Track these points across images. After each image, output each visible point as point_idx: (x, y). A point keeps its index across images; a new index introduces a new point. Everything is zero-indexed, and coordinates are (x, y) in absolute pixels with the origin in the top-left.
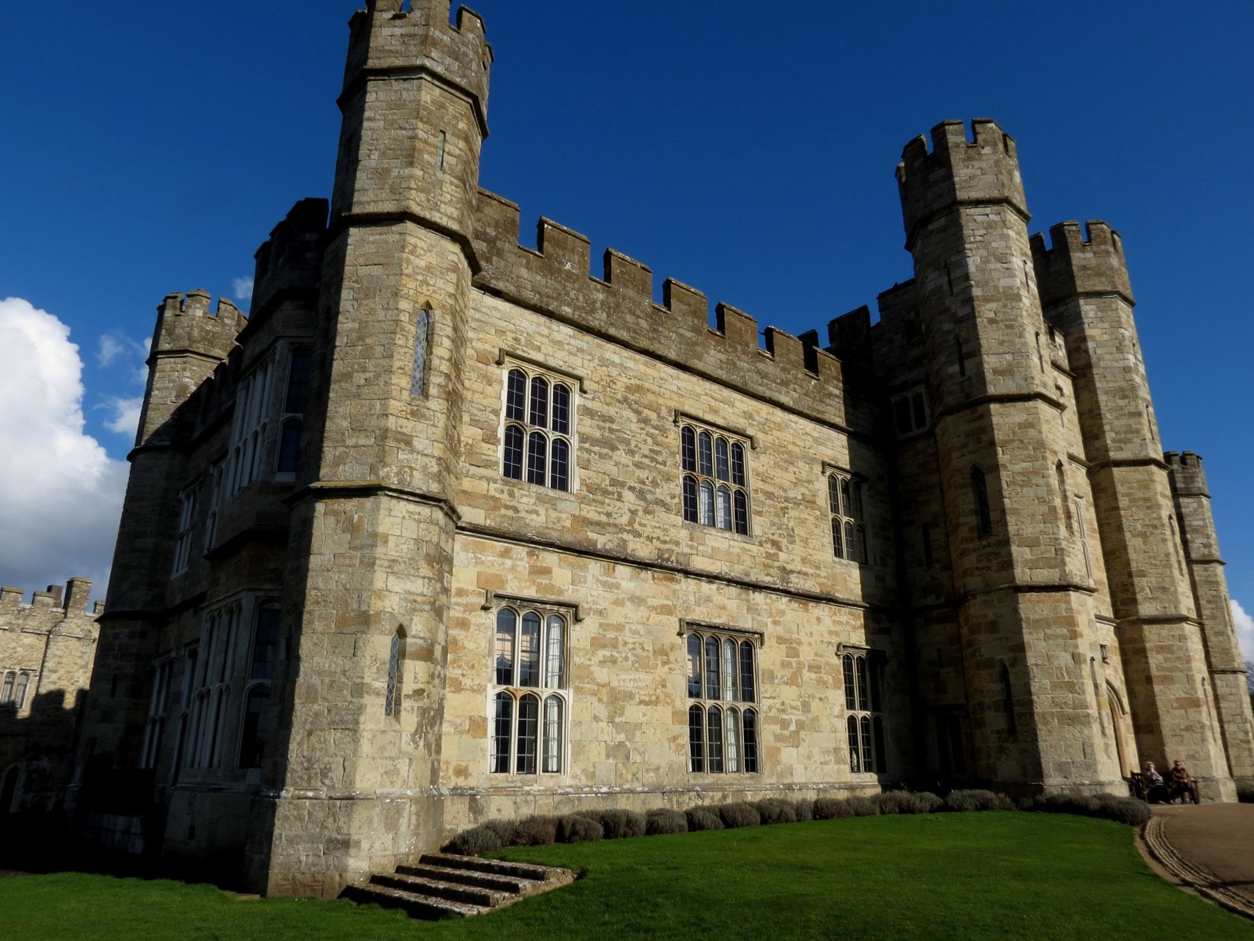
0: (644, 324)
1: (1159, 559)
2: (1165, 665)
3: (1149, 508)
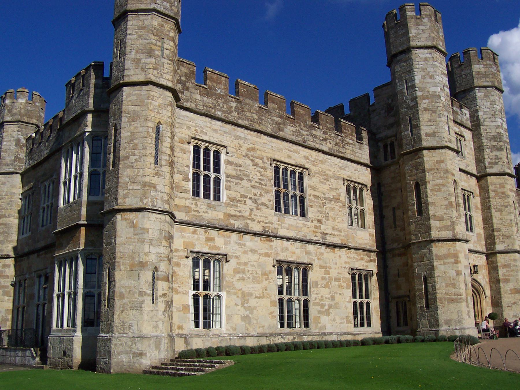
0: (255, 117)
1: (507, 222)
2: (506, 274)
3: (504, 197)
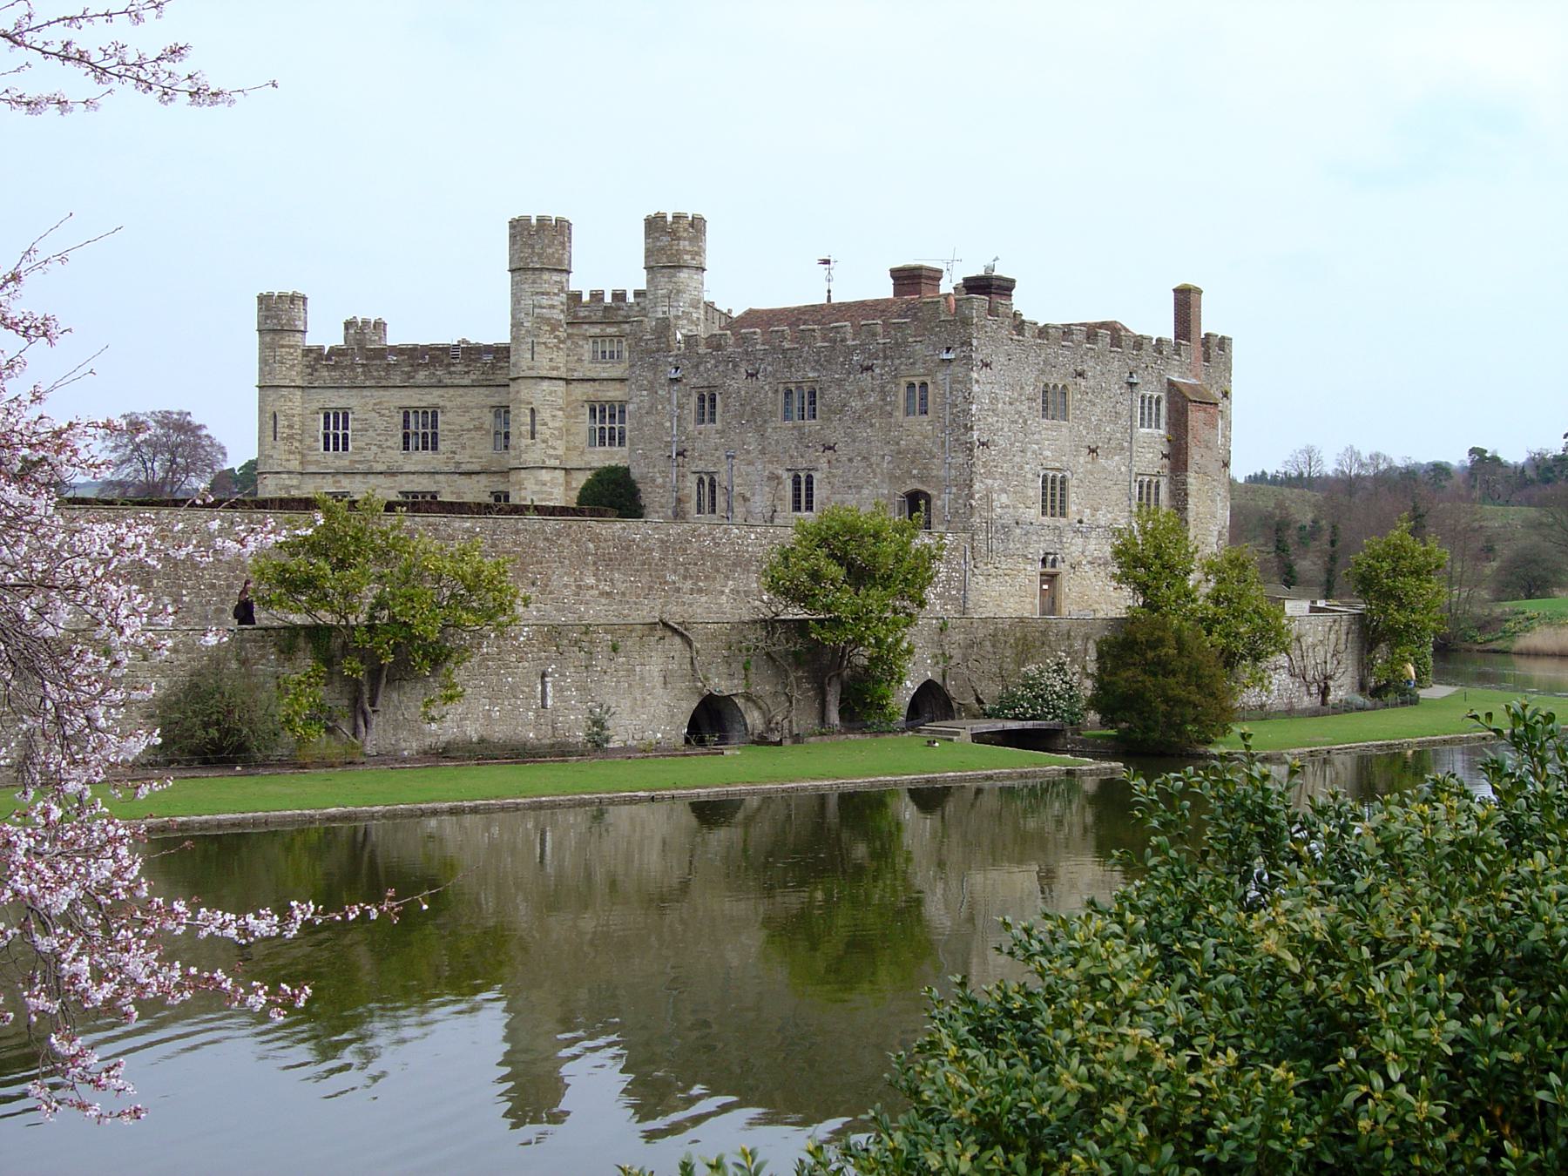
0: (383, 373)
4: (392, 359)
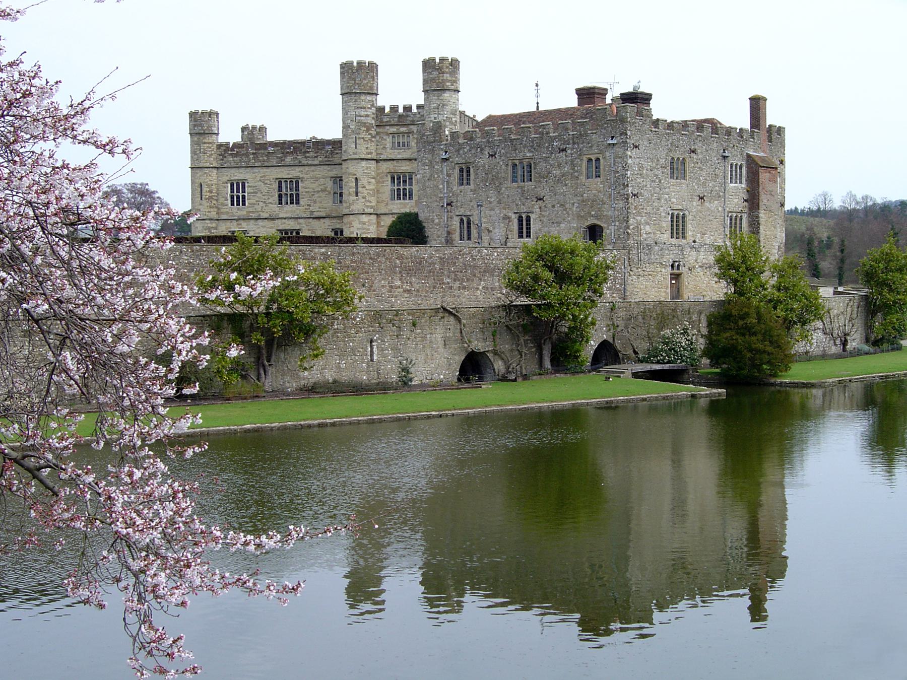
0: (265, 158)
4: (271, 149)
